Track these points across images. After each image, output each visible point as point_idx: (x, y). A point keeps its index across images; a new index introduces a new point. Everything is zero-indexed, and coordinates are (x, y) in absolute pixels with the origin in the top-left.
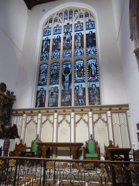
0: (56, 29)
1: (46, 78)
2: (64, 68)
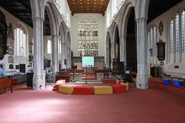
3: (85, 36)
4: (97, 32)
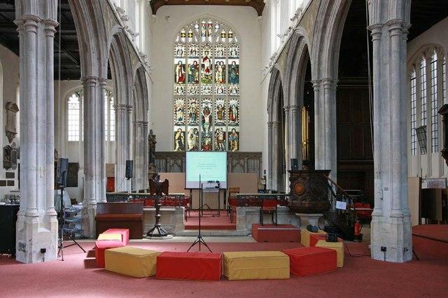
3: (197, 82)
4: (237, 68)
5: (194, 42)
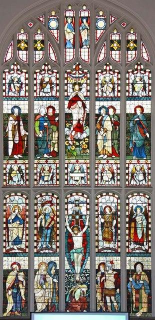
0: (42, 80)
1: (24, 237)
2: (70, 212)
3: (55, 155)
5: (46, 61)
